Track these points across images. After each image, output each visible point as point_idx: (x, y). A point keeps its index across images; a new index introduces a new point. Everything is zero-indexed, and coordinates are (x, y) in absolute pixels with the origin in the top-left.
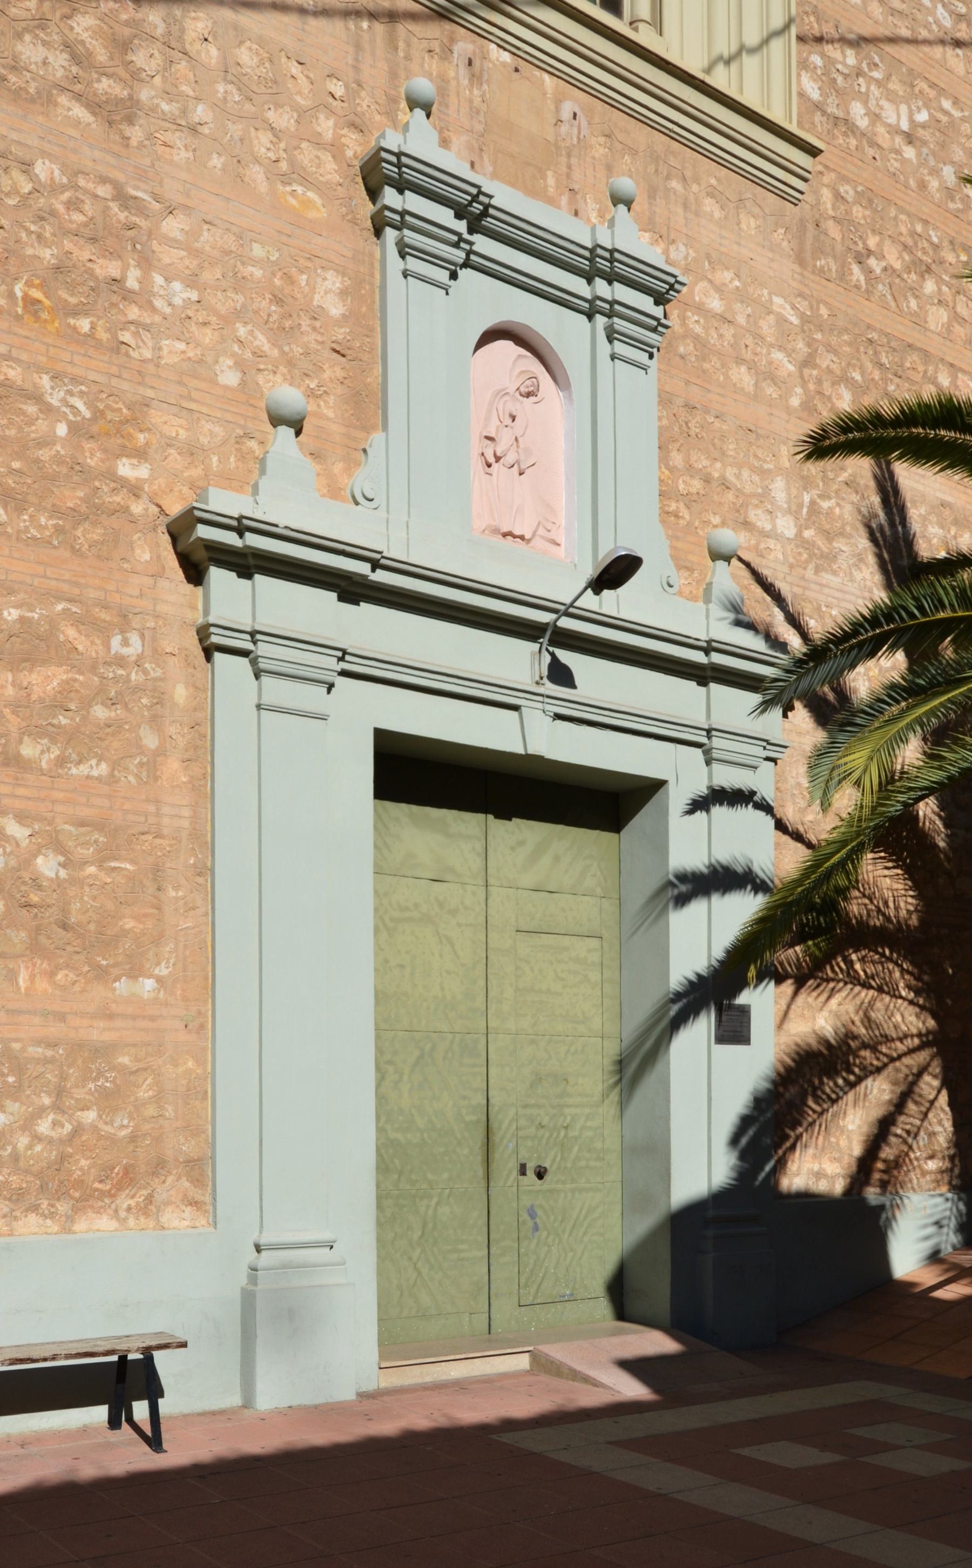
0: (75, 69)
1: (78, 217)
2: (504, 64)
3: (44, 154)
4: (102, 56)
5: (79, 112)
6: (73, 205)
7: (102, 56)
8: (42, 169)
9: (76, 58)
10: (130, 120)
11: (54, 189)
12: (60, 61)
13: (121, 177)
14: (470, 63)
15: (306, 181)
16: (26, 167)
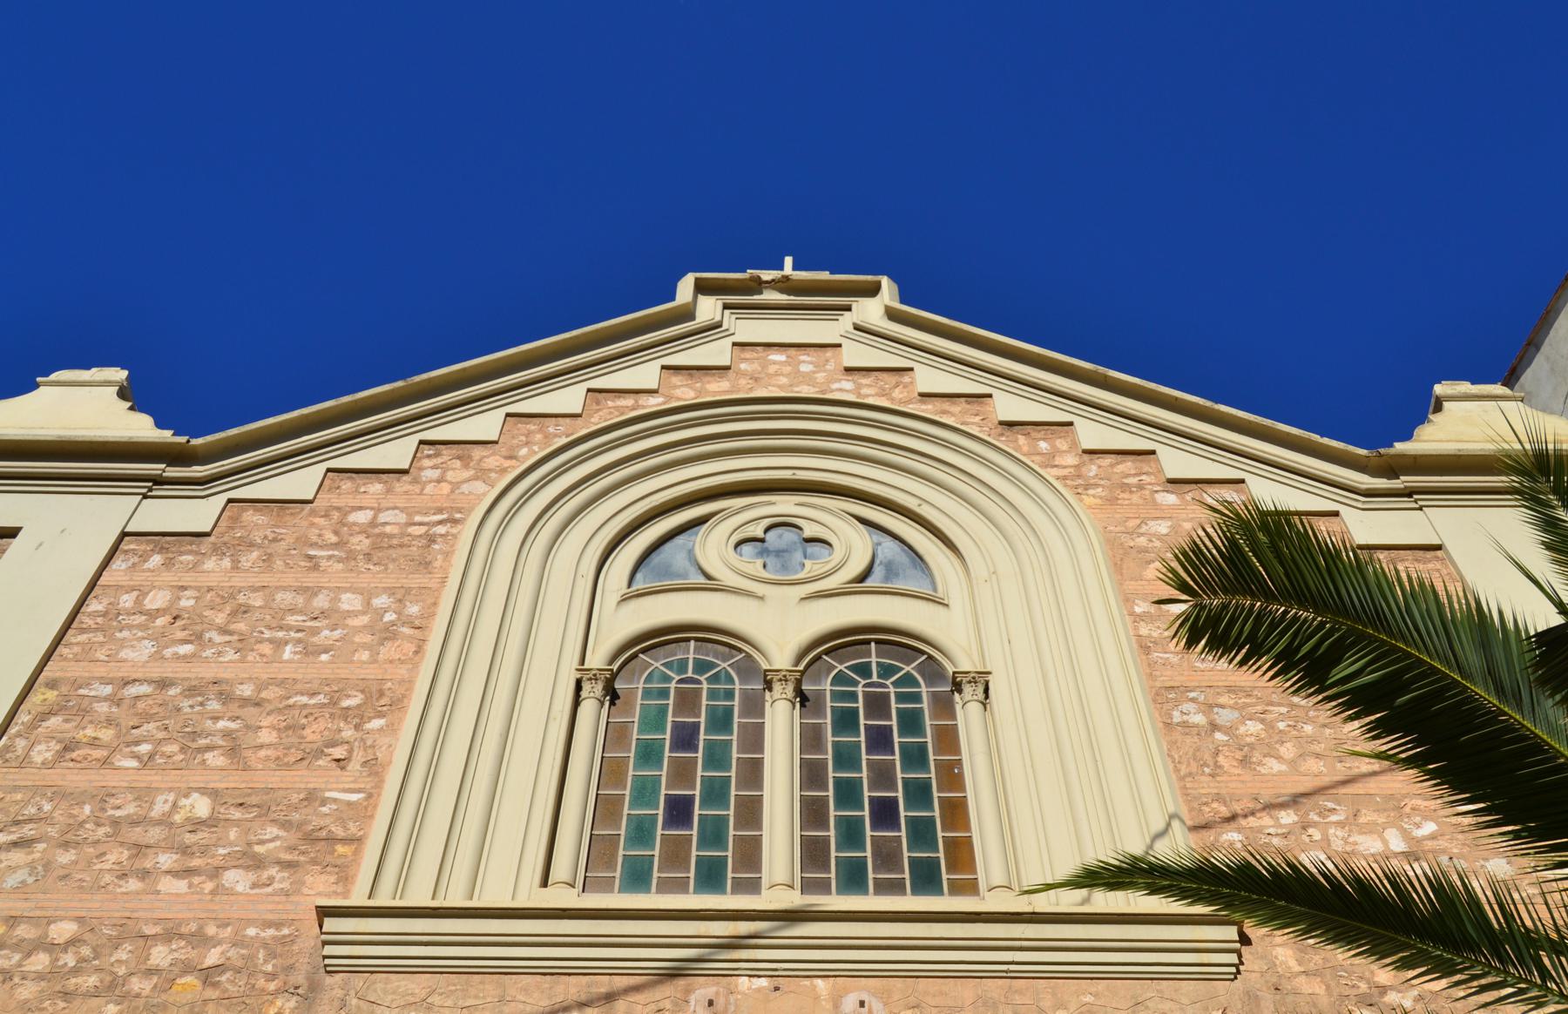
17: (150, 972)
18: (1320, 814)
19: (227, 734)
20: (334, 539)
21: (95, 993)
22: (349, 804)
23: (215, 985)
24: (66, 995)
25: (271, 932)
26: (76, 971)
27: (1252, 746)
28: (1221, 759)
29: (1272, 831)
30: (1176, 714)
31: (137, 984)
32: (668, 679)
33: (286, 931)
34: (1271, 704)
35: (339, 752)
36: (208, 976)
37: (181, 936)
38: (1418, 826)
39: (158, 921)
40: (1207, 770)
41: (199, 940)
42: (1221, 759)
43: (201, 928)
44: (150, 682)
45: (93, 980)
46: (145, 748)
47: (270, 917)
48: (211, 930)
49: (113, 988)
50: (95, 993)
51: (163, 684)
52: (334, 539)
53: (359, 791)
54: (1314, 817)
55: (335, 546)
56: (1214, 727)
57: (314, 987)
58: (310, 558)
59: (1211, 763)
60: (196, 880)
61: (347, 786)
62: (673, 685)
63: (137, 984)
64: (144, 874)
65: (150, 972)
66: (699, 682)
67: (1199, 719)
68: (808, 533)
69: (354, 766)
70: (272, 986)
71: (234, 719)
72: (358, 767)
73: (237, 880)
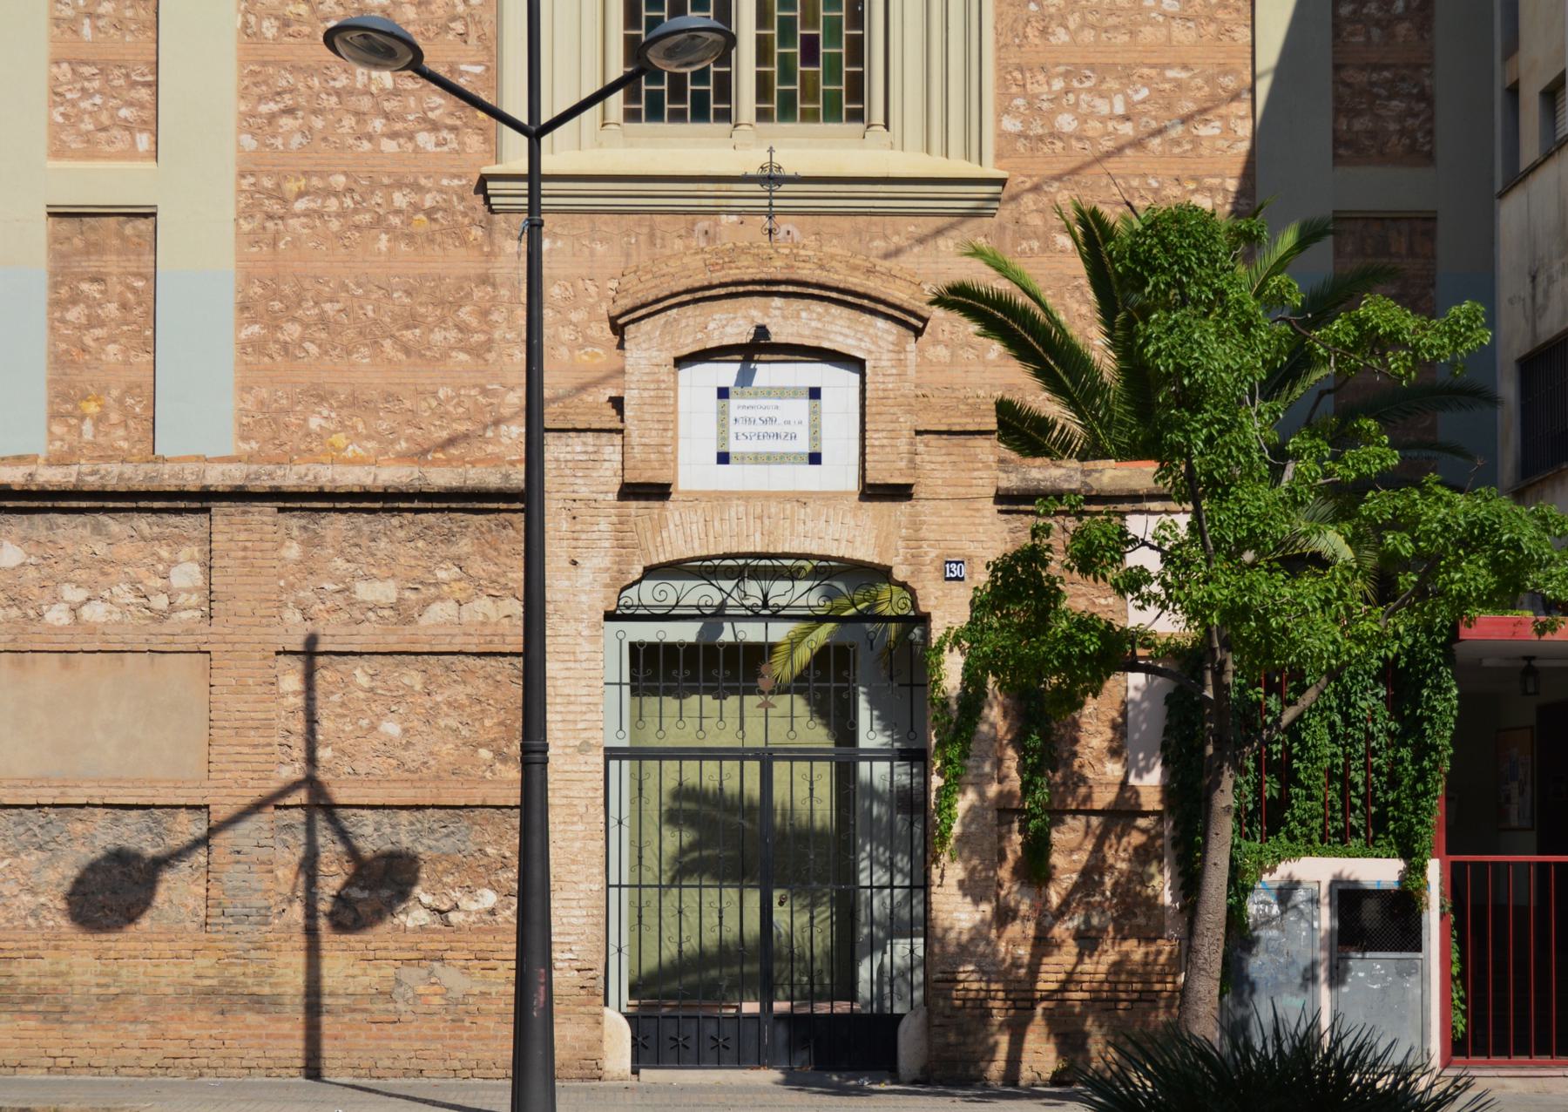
0: (460, 336)
1: (461, 410)
2: (732, 223)
3: (443, 384)
4: (474, 322)
6: (459, 404)
7: (474, 322)
8: (441, 394)
9: (461, 330)
10: (489, 351)
11: (449, 399)
12: (453, 335)
13: (483, 381)
14: (706, 232)
15: (593, 345)
16: (434, 394)
17: (398, 212)
18: (1081, 82)
21: (371, 226)
22: (476, 75)
23: (435, 220)
25: (456, 182)
26: (356, 211)
27: (1051, 17)
28: (1029, 30)
29: (1044, 97)
31: (395, 221)
35: (459, 27)
36: (430, 213)
37: (407, 186)
38: (1136, 91)
39: (389, 175)
40: (1017, 41)
41: (418, 188)
42: (1029, 30)
43: (416, 179)
45: (366, 218)
47: (454, 170)
48: (423, 181)
49: (378, 222)
50: (371, 226)
53: (479, 63)
54: (1076, 84)
59: (1021, 34)
60: (402, 141)
61: (473, 59)
64: (370, 138)
69: (472, 40)
70: (466, 221)
72: (475, 42)
73: (425, 139)
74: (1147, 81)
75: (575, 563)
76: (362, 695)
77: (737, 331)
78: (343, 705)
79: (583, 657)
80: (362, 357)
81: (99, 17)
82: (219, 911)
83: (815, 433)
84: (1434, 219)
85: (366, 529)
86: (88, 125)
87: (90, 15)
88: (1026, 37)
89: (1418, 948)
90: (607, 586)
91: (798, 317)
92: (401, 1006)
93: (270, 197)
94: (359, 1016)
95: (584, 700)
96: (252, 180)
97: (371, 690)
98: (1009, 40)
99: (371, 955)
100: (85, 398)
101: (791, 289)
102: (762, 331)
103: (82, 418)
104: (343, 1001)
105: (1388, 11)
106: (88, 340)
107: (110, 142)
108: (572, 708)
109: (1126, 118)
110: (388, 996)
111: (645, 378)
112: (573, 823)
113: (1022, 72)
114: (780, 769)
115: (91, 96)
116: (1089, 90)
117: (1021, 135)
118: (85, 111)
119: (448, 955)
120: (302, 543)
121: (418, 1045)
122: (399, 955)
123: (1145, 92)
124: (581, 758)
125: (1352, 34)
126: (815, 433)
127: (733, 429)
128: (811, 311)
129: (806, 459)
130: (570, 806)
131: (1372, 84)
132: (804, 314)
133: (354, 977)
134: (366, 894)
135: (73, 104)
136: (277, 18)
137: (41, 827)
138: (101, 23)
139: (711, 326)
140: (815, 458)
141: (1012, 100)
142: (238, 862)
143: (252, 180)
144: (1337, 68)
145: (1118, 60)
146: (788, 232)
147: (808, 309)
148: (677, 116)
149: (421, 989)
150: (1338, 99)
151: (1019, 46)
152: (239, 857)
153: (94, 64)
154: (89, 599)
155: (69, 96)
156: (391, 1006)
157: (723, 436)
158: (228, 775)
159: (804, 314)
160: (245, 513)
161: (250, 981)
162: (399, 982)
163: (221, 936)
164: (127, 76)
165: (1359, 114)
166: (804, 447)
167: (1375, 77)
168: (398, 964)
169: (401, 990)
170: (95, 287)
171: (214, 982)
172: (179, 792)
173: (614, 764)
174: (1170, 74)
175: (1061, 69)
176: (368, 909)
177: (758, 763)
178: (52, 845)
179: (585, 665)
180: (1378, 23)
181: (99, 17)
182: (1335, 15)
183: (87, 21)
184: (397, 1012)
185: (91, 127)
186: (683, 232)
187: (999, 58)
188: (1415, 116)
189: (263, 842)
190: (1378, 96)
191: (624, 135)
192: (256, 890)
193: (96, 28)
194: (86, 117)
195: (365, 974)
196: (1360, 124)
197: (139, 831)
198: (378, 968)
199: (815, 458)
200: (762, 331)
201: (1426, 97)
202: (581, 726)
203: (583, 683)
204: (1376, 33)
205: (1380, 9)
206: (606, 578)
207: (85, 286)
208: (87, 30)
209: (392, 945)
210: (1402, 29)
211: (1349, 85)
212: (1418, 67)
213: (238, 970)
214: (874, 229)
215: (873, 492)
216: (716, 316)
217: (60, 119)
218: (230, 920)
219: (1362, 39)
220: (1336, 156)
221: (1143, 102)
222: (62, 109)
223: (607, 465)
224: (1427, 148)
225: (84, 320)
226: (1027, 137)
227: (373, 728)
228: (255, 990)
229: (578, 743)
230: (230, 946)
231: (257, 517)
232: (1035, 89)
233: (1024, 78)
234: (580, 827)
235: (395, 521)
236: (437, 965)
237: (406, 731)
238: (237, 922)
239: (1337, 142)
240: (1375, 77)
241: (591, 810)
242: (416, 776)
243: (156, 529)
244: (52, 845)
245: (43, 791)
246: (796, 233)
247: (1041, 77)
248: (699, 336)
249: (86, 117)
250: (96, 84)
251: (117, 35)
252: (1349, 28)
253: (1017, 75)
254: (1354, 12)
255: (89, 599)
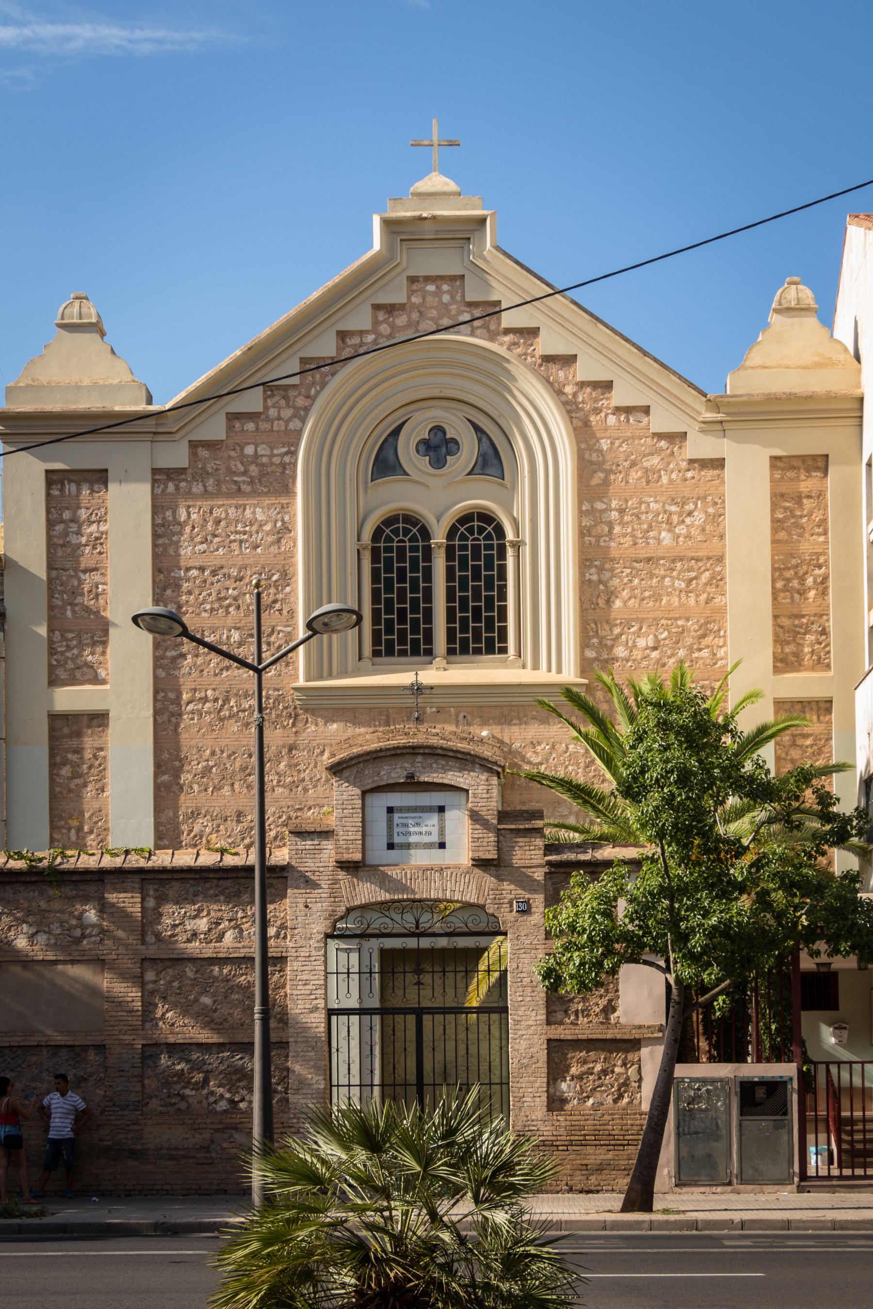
2: (433, 712)
5: (281, 790)
17: (244, 711)
19: (235, 599)
20: (242, 469)
24: (221, 720)
30: (587, 575)
32: (392, 541)
33: (281, 693)
34: (625, 568)
44: (196, 568)
46: (208, 607)
51: (202, 569)
52: (242, 469)
55: (245, 473)
56: (600, 582)
57: (297, 716)
58: (236, 482)
62: (395, 544)
63: (241, 715)
65: (244, 711)
66: (405, 542)
67: (595, 578)
68: (448, 436)
69: (285, 612)
71: (234, 589)
74: (667, 628)
75: (307, 907)
76: (189, 982)
77: (396, 775)
78: (180, 988)
79: (313, 958)
80: (226, 791)
81: (76, 605)
82: (111, 1104)
83: (442, 832)
84: (831, 701)
85: (191, 890)
86: (70, 665)
87: (71, 604)
88: (598, 604)
89: (785, 1113)
90: (325, 919)
91: (431, 766)
92: (214, 1155)
93: (172, 704)
94: (191, 1161)
95: (314, 982)
96: (163, 694)
97: (195, 979)
98: (588, 607)
99: (197, 1127)
100: (70, 817)
101: (426, 751)
102: (411, 776)
103: (69, 829)
104: (183, 1153)
105: (803, 584)
106: (72, 786)
107: (83, 675)
108: (307, 987)
109: (655, 648)
110: (207, 1149)
111: (345, 802)
112: (308, 1051)
113: (596, 624)
114: (427, 1019)
115: (73, 649)
116: (634, 633)
117: (596, 659)
118: (68, 658)
119: (239, 1126)
120: (156, 898)
121: (224, 1176)
122: (213, 1126)
123: (666, 634)
124: (312, 1015)
125: (784, 598)
126: (442, 832)
127: (396, 830)
128: (438, 764)
129: (437, 846)
130: (307, 1042)
131: (796, 626)
132: (434, 765)
133: (187, 1139)
134: (194, 1092)
135: (62, 653)
136: (175, 603)
137: (12, 1059)
138: (77, 608)
139: (382, 773)
140: (442, 845)
141: (590, 639)
142: (122, 1076)
143: (163, 694)
144: (775, 617)
145: (650, 616)
146: (465, 717)
147: (436, 762)
148: (403, 653)
149: (225, 1145)
150: (776, 635)
151: (594, 609)
152: (122, 1073)
153: (72, 631)
154: (37, 932)
155: (59, 649)
156: (208, 1155)
157: (390, 835)
158: (116, 1028)
159: (434, 765)
160: (123, 882)
161: (129, 1142)
162: (212, 1142)
163: (113, 1118)
164: (92, 637)
165: (788, 643)
166: (435, 838)
167: (796, 622)
168: (212, 1131)
169: (214, 1146)
170: (76, 756)
171: (110, 1143)
172: (88, 1038)
173: (334, 1018)
174: (680, 623)
175: (618, 622)
176: (195, 1101)
177: (414, 1016)
178: (19, 1069)
179: (314, 963)
180: (799, 592)
181: (76, 605)
182: (773, 587)
183: (69, 608)
184: (211, 1158)
185: (72, 666)
186: (405, 718)
187: (583, 616)
188: (820, 643)
189: (135, 1065)
190: (799, 633)
191: (373, 665)
192: (132, 1092)
193: (74, 612)
194: (69, 661)
195: (194, 1137)
196: (787, 650)
197: (67, 1061)
198: (201, 1134)
199: (442, 845)
200: (411, 776)
201: (824, 632)
202: (313, 997)
203: (314, 973)
204: (796, 596)
205: (800, 583)
206: (326, 914)
207: (70, 756)
208: (69, 614)
209: (209, 1121)
210: (812, 594)
211: (782, 627)
212: (822, 615)
213: (123, 1136)
214: (513, 714)
215: (481, 864)
216: (386, 767)
217: (55, 663)
218: (116, 1109)
219: (789, 600)
220: (774, 667)
221: (665, 639)
222: (55, 657)
223: (325, 851)
224: (826, 661)
225: (69, 774)
226: (599, 660)
227: (196, 1000)
228: (132, 1147)
229: (311, 1007)
230: (118, 1123)
231: (130, 884)
232: (603, 633)
233: (597, 627)
234: (313, 1054)
235: (208, 885)
236: (233, 1131)
237: (215, 1002)
238: (123, 1109)
239: (776, 659)
240: (796, 622)
241: (319, 1044)
242: (221, 1027)
243: (74, 892)
244: (19, 1069)
245: (13, 1039)
246: (469, 717)
247: (607, 627)
248: (376, 778)
249: (69, 661)
250: (74, 642)
251: (86, 615)
252: (782, 595)
253: (593, 625)
254: (785, 586)
255: (37, 932)
